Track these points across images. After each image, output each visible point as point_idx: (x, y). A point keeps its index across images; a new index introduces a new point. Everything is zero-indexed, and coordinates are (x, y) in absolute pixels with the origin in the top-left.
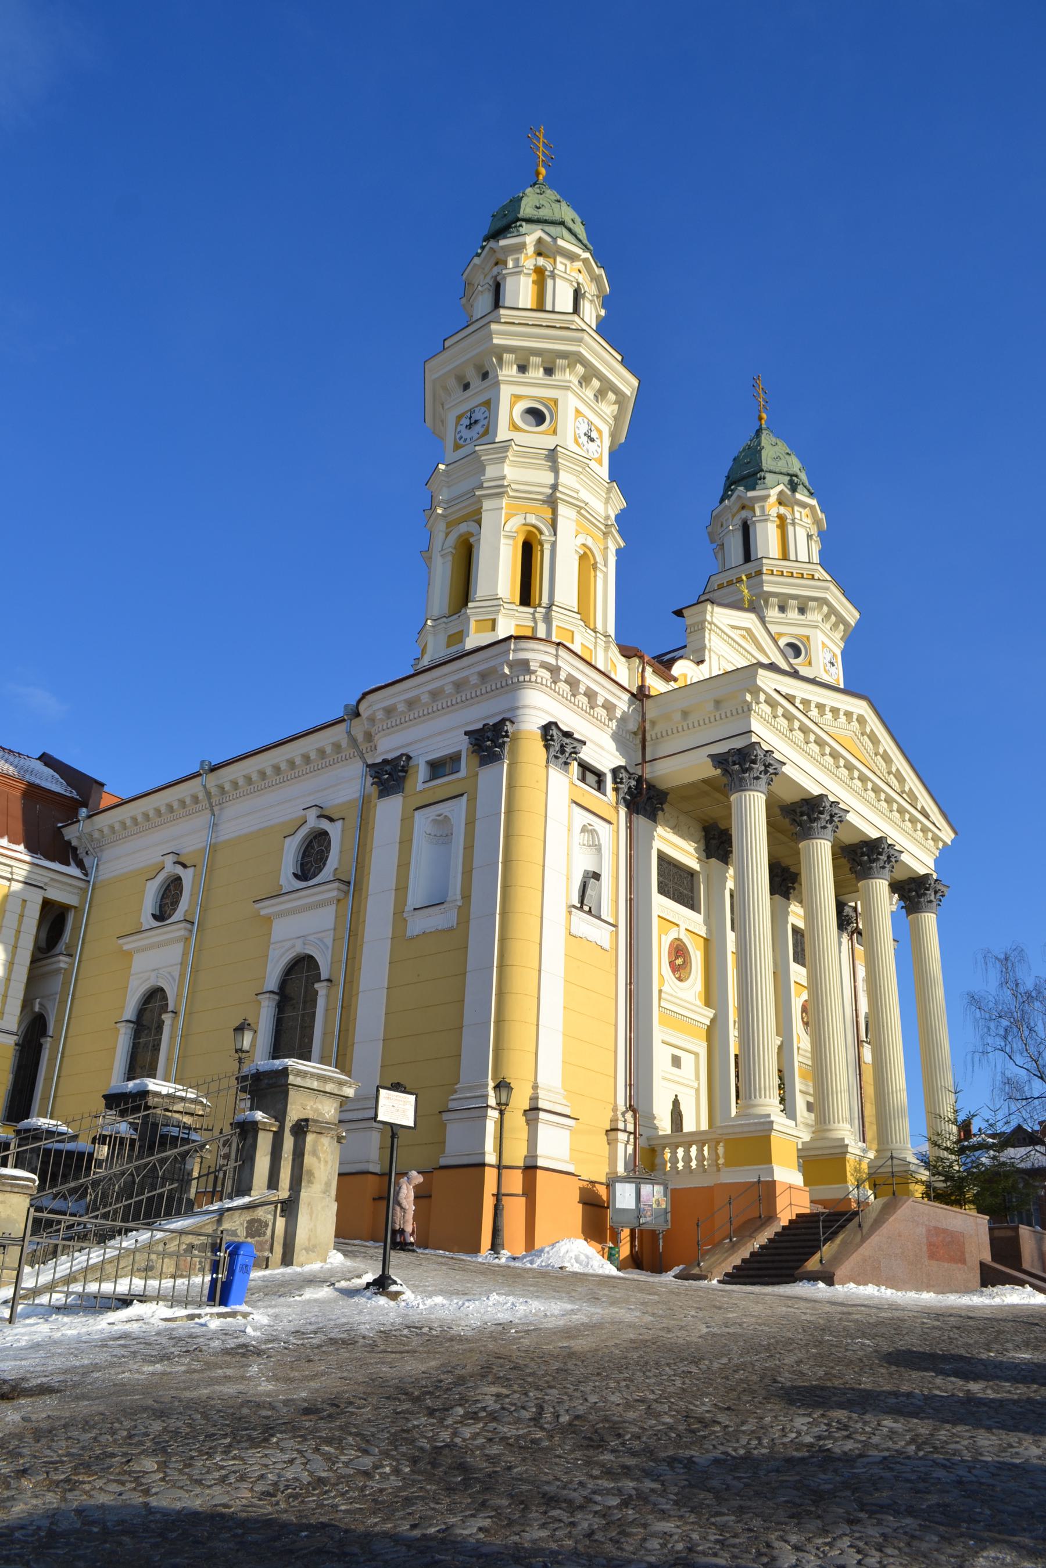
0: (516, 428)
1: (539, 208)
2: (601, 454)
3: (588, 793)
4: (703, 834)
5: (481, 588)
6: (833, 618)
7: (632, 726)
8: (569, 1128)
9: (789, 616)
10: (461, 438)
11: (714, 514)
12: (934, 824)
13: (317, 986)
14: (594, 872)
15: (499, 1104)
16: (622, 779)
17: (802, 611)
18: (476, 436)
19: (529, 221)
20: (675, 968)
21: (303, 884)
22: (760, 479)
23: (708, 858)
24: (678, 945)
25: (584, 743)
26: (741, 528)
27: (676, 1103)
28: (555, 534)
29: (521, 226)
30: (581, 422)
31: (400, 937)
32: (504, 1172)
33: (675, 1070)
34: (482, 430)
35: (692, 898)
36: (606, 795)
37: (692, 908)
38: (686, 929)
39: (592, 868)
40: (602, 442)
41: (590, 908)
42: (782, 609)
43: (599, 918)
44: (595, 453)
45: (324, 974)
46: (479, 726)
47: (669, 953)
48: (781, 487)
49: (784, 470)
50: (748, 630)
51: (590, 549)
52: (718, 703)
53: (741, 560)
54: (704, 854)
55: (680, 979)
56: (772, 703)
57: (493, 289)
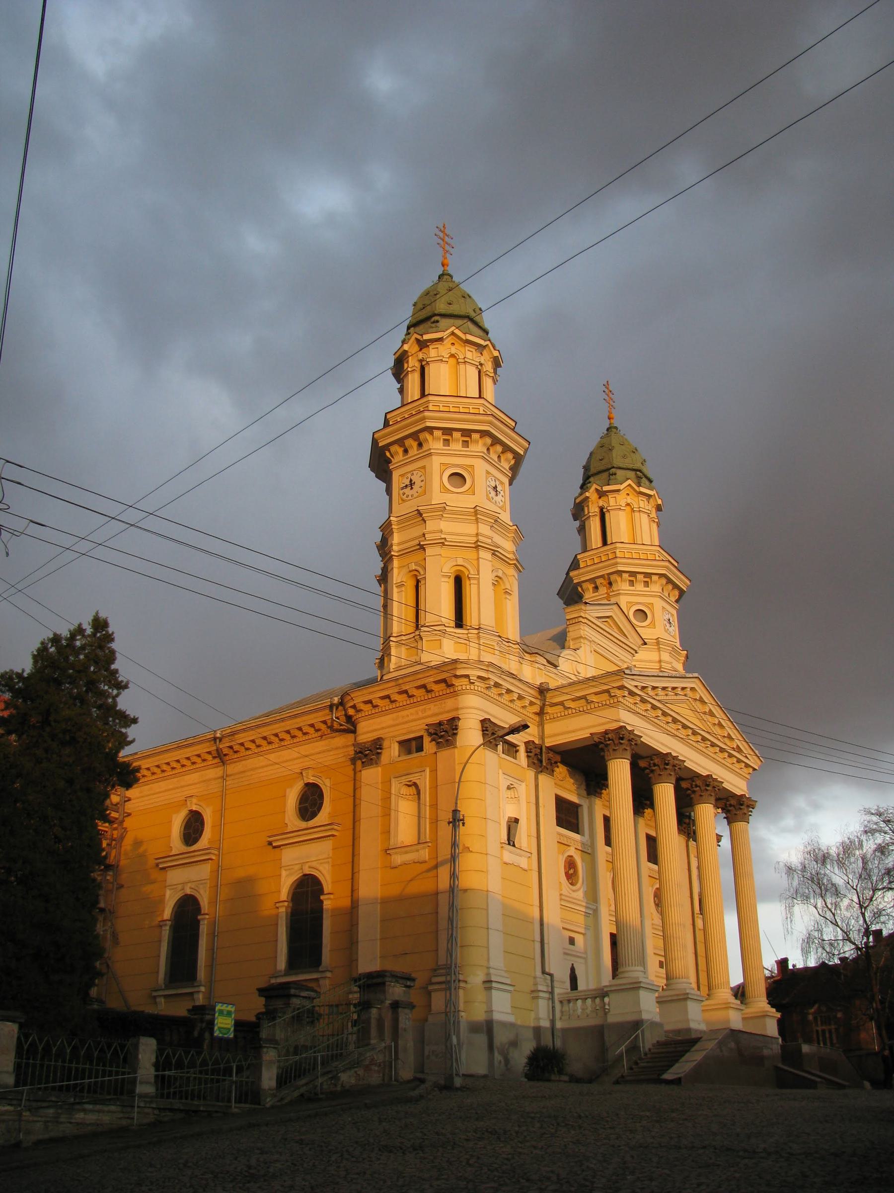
1: (450, 304)
2: (505, 502)
5: (428, 619)
7: (536, 709)
10: (404, 494)
11: (578, 501)
12: (746, 757)
13: (322, 897)
14: (516, 818)
17: (646, 584)
18: (416, 495)
20: (569, 876)
21: (304, 825)
22: (612, 475)
24: (571, 860)
26: (598, 514)
27: (573, 970)
28: (478, 574)
29: (437, 322)
30: (491, 480)
34: (420, 490)
35: (578, 824)
38: (576, 849)
39: (514, 815)
40: (504, 492)
41: (514, 842)
42: (632, 583)
44: (501, 502)
45: (326, 889)
46: (435, 720)
47: (565, 866)
48: (629, 482)
49: (631, 466)
50: (608, 617)
51: (500, 578)
53: (600, 544)
54: (585, 793)
55: (572, 884)
57: (418, 369)
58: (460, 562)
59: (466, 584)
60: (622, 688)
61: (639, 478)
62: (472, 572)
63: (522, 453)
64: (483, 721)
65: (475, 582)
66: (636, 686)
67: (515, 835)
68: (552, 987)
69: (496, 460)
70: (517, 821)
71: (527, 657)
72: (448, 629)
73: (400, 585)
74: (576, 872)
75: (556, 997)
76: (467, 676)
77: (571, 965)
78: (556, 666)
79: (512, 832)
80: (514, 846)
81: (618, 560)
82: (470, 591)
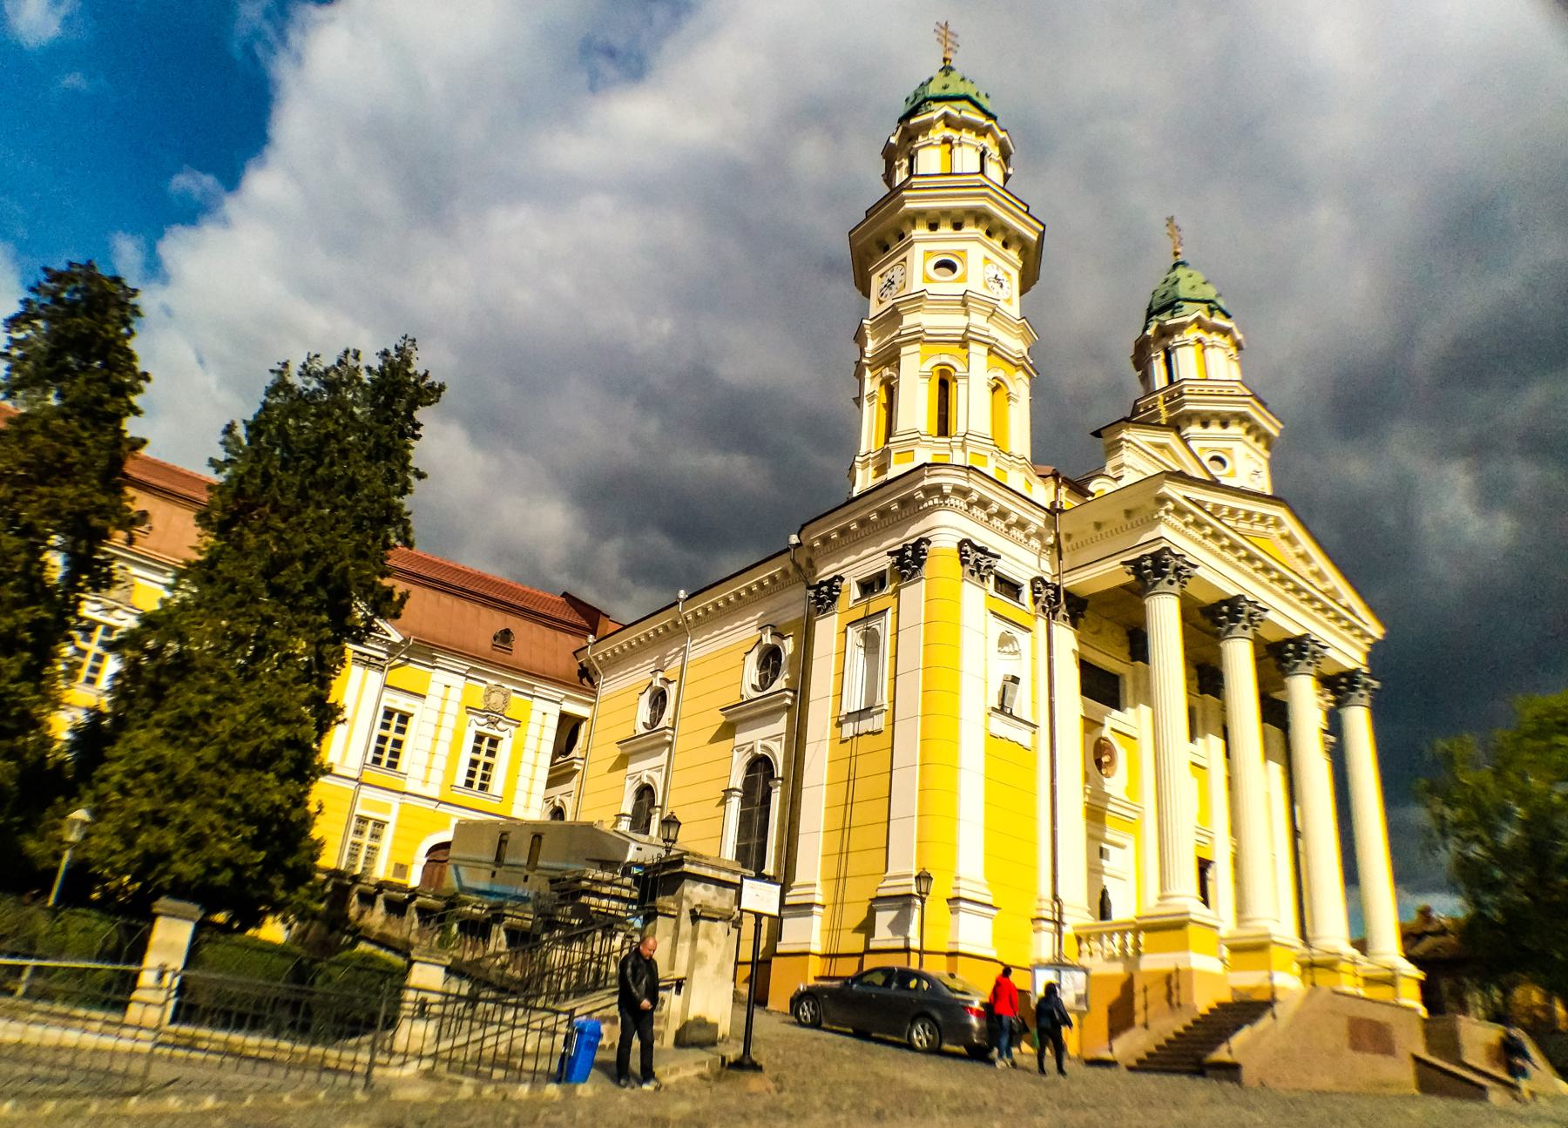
0: (931, 280)
3: (1005, 605)
4: (1126, 638)
5: (903, 423)
8: (991, 917)
12: (1359, 618)
15: (920, 892)
17: (1224, 425)
19: (938, 99)
23: (1134, 660)
32: (925, 956)
52: (1128, 513)
53: (1165, 383)
54: (1129, 658)
56: (1180, 512)
58: (945, 359)
60: (1162, 500)
61: (1211, 310)
62: (960, 368)
63: (1034, 237)
64: (961, 544)
65: (965, 381)
66: (1186, 498)
67: (1012, 700)
68: (1060, 914)
69: (999, 244)
70: (1015, 680)
72: (923, 438)
73: (872, 396)
75: (1067, 931)
79: (1008, 695)
81: (1185, 397)
82: (959, 393)
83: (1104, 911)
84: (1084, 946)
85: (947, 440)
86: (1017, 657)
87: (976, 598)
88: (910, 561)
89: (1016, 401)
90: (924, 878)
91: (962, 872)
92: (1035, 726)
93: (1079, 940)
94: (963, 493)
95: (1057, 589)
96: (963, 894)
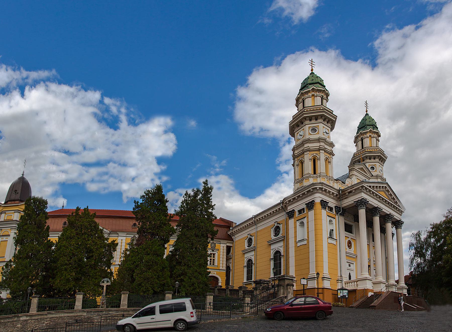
3: (331, 214)
6: (381, 160)
7: (338, 196)
8: (330, 281)
9: (372, 160)
14: (332, 229)
16: (336, 208)
25: (329, 203)
27: (350, 274)
28: (320, 158)
31: (296, 247)
32: (319, 289)
33: (349, 267)
36: (333, 213)
37: (352, 233)
43: (334, 239)
46: (308, 202)
47: (348, 243)
50: (362, 168)
55: (350, 249)
59: (316, 160)
67: (332, 234)
70: (333, 230)
71: (336, 181)
74: (351, 245)
76: (316, 188)
77: (349, 273)
78: (344, 183)
79: (331, 234)
80: (332, 237)
82: (318, 163)
83: (350, 278)
84: (346, 285)
85: (316, 175)
86: (332, 225)
87: (324, 213)
88: (311, 206)
89: (330, 163)
90: (318, 274)
91: (324, 272)
92: (336, 240)
93: (345, 283)
94: (321, 189)
95: (340, 208)
96: (325, 276)
